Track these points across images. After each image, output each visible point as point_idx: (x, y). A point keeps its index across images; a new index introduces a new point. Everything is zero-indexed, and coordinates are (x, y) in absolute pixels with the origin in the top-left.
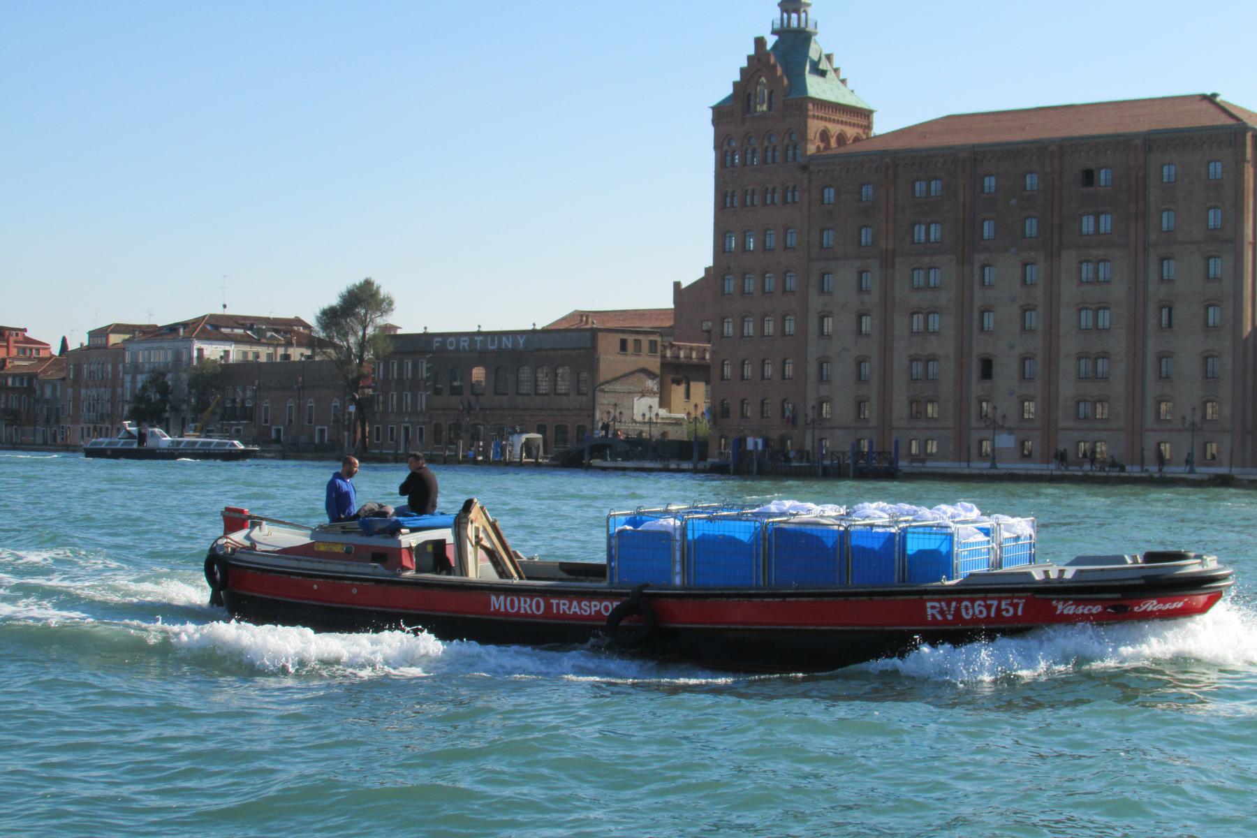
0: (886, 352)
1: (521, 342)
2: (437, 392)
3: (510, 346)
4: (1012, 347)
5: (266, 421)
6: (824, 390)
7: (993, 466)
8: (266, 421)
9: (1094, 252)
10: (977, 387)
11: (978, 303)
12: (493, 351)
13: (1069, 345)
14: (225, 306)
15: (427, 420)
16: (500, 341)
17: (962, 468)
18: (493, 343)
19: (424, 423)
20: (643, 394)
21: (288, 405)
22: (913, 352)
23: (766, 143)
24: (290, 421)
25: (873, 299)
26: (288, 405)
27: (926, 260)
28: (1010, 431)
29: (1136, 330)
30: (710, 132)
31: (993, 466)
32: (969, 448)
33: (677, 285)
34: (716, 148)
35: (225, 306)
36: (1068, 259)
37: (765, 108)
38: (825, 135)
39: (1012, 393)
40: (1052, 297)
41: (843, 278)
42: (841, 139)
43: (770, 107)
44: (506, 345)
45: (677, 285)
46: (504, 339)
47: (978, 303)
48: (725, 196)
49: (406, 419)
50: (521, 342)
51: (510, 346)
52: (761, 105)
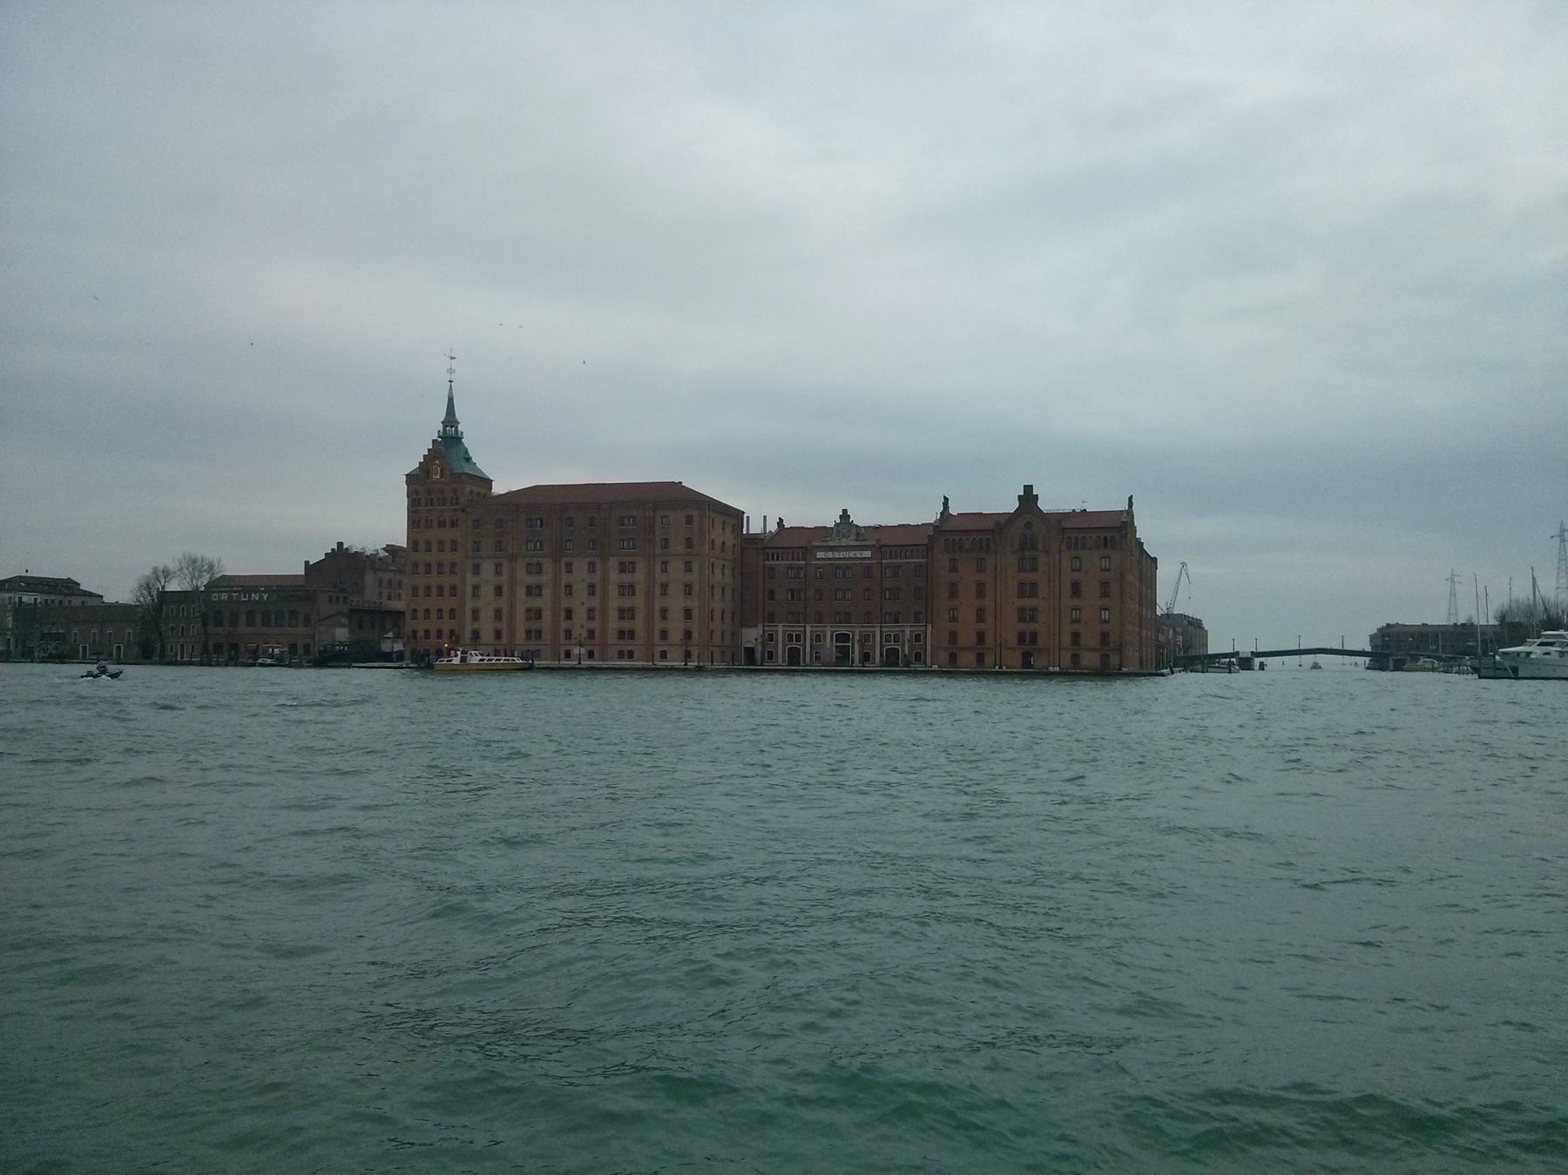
0: (512, 606)
3: (257, 599)
6: (476, 626)
7: (580, 663)
9: (626, 558)
10: (564, 625)
11: (563, 583)
13: (614, 602)
14: (27, 571)
16: (250, 596)
17: (555, 664)
18: (245, 597)
20: (342, 626)
22: (528, 606)
23: (439, 496)
25: (504, 579)
27: (535, 560)
28: (581, 645)
29: (649, 596)
30: (403, 488)
31: (580, 663)
32: (559, 654)
33: (307, 563)
34: (408, 496)
35: (27, 571)
36: (613, 563)
37: (438, 477)
38: (471, 491)
39: (582, 627)
40: (605, 580)
41: (487, 568)
42: (478, 494)
43: (442, 476)
45: (307, 563)
47: (563, 583)
48: (414, 521)
52: (436, 475)
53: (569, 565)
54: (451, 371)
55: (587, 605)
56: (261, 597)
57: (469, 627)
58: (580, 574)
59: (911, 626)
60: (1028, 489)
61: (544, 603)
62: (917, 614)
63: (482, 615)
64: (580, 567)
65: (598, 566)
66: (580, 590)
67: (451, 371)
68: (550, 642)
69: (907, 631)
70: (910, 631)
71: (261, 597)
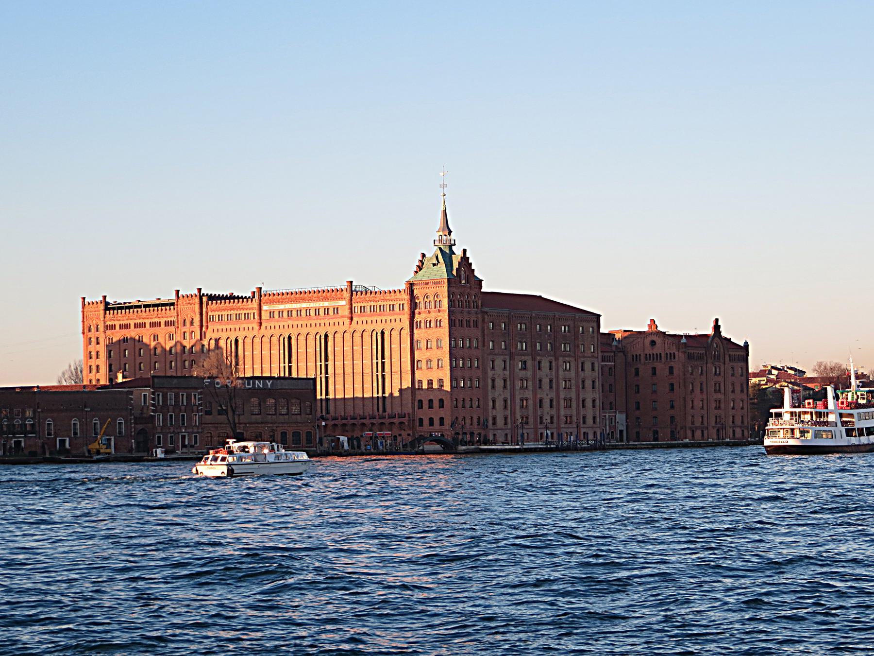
0: (513, 396)
1: (269, 384)
2: (208, 413)
3: (261, 386)
4: (547, 395)
5: (49, 434)
8: (49, 434)
12: (249, 389)
15: (200, 430)
16: (254, 384)
18: (249, 384)
19: (198, 432)
21: (73, 422)
24: (75, 434)
25: (507, 373)
26: (73, 422)
27: (523, 357)
44: (258, 385)
46: (257, 382)
49: (184, 430)
50: (269, 384)
51: (261, 386)
53: (539, 362)
54: (444, 186)
55: (549, 396)
56: (265, 384)
57: (491, 413)
58: (545, 373)
59: (609, 413)
60: (717, 320)
61: (529, 394)
62: (611, 403)
63: (497, 404)
64: (545, 364)
65: (554, 364)
66: (546, 381)
67: (444, 186)
68: (532, 427)
69: (607, 415)
70: (609, 416)
71: (265, 384)
